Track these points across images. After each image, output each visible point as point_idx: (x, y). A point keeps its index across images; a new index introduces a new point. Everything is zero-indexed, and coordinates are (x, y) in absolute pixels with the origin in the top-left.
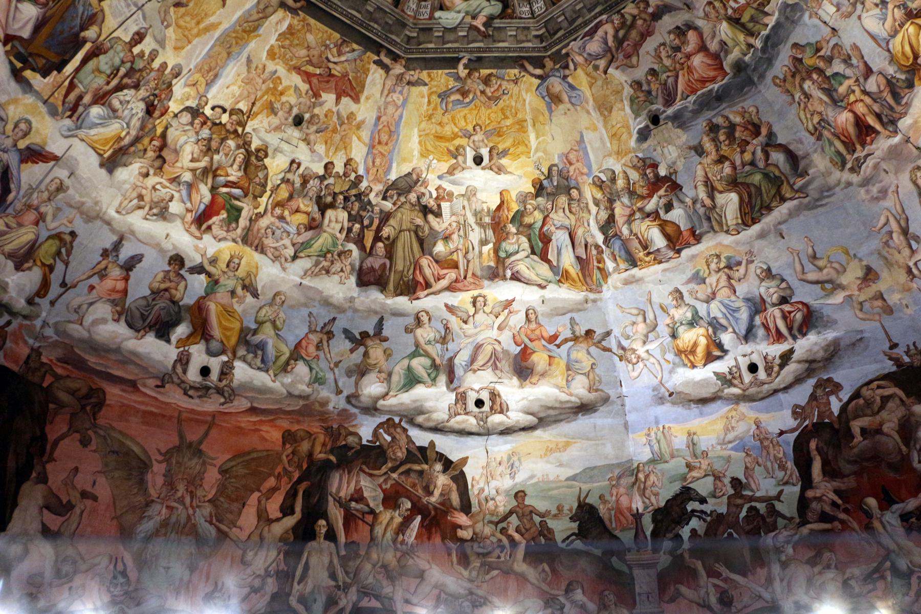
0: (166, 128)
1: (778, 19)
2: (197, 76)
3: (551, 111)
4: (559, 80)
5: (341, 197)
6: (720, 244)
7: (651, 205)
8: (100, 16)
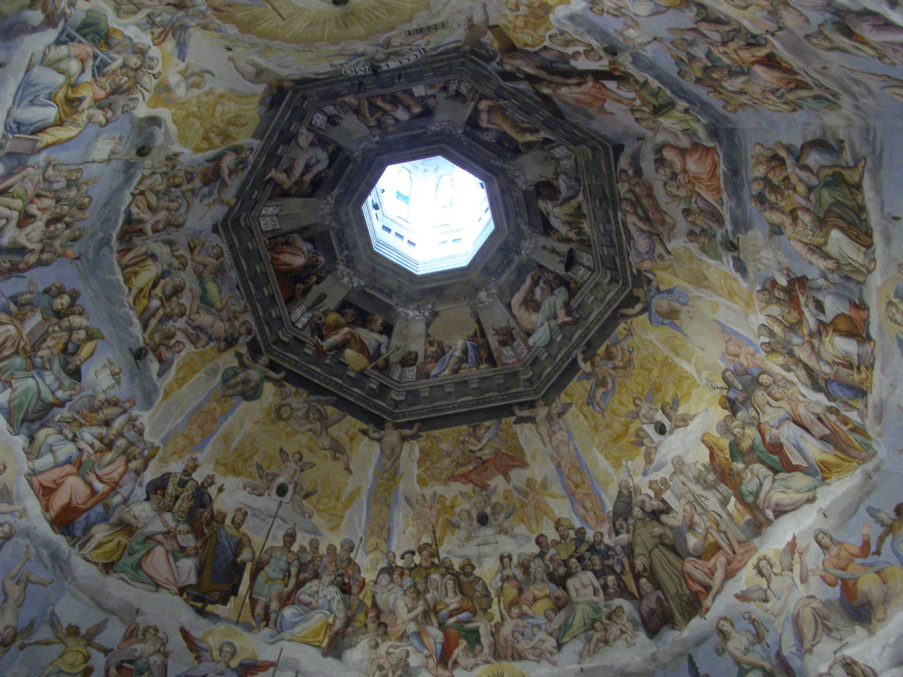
0: (374, 597)
1: (651, 75)
2: (373, 540)
3: (678, 328)
4: (658, 297)
5: (574, 560)
6: (879, 290)
7: (811, 321)
8: (245, 540)
